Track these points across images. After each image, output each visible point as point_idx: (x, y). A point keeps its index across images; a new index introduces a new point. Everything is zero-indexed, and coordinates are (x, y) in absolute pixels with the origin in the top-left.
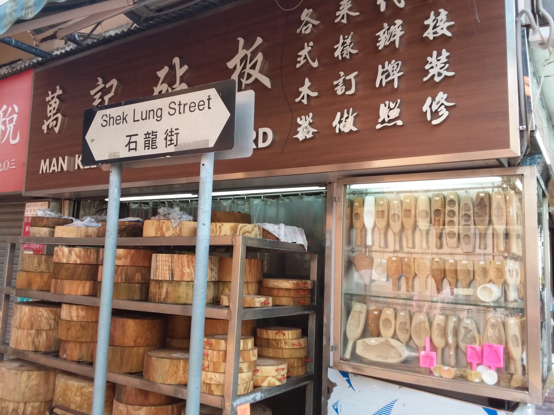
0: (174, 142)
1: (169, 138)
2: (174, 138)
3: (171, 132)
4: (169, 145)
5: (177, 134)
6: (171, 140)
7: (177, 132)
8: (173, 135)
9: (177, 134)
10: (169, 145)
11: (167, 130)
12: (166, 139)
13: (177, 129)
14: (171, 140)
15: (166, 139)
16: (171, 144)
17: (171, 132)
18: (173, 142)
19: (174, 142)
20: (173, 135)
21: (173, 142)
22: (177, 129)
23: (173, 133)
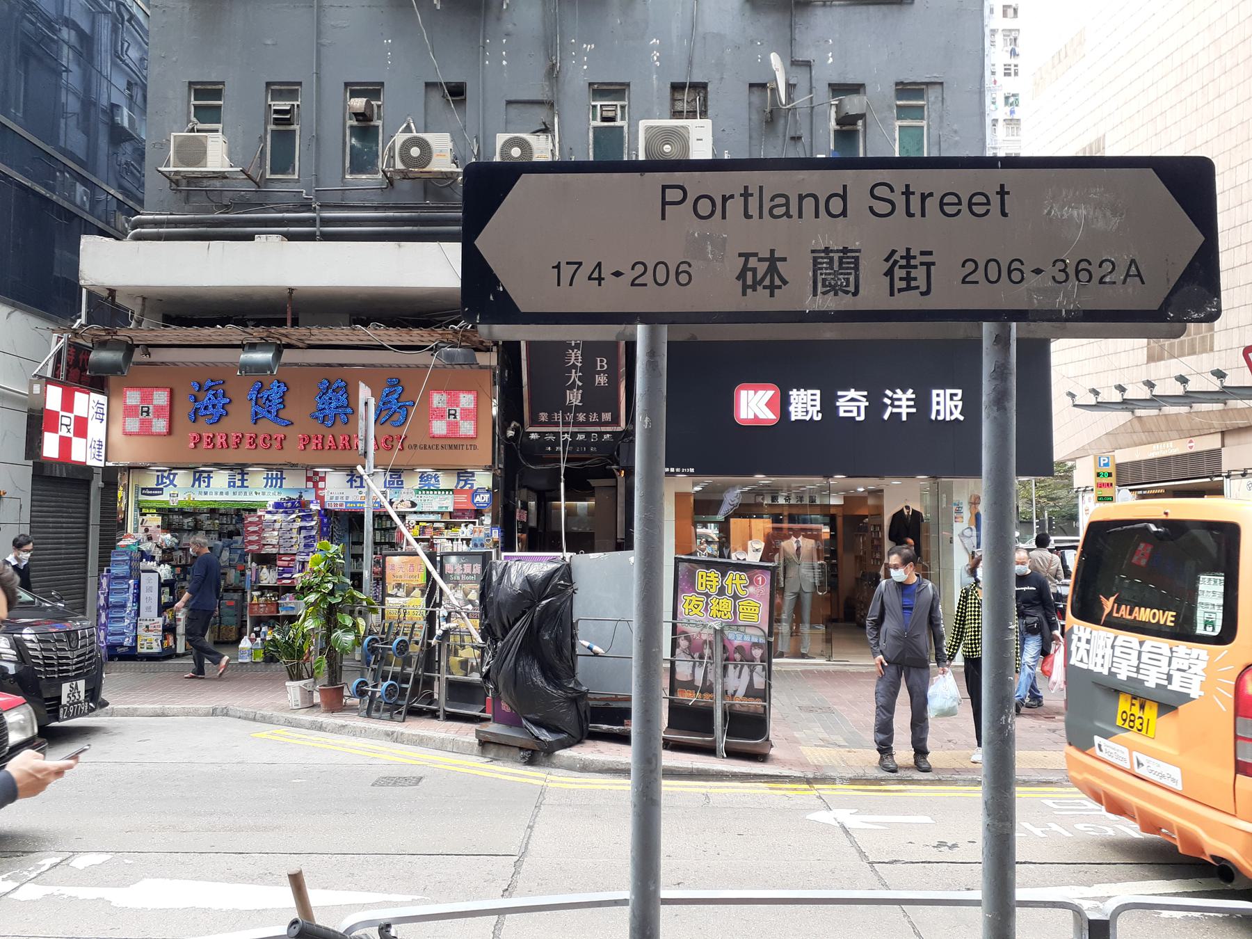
1: (899, 273)
2: (920, 273)
3: (908, 256)
4: (900, 290)
5: (929, 265)
6: (908, 279)
8: (915, 267)
9: (929, 265)
10: (900, 290)
11: (894, 252)
12: (890, 273)
14: (908, 279)
16: (909, 288)
17: (908, 256)
18: (913, 284)
20: (915, 267)
21: (913, 284)
23: (913, 262)
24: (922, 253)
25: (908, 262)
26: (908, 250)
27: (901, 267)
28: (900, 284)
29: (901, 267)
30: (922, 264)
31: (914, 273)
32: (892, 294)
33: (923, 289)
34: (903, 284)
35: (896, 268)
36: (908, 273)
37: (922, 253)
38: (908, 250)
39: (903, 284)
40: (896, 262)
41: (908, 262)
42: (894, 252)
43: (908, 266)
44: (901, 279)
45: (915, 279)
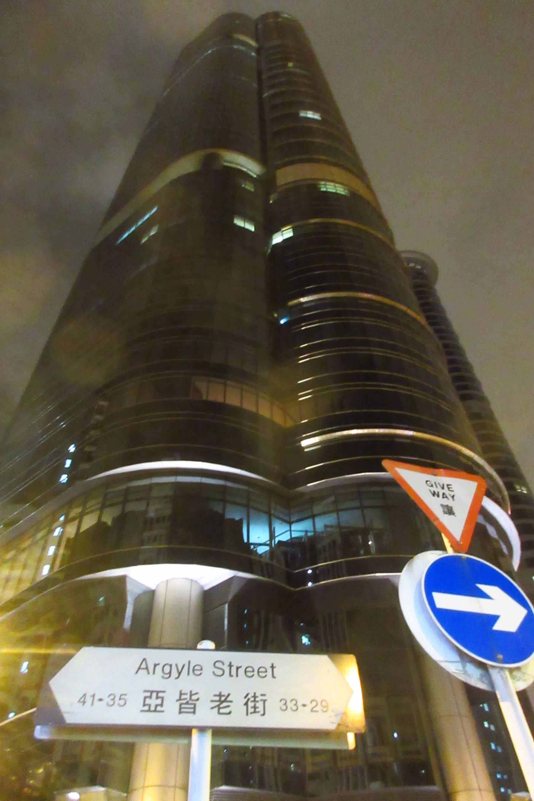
1: (251, 704)
2: (260, 705)
3: (255, 697)
4: (251, 713)
6: (255, 707)
7: (263, 698)
8: (258, 702)
9: (264, 701)
10: (251, 713)
11: (247, 695)
12: (246, 704)
15: (246, 704)
17: (255, 697)
18: (257, 710)
20: (258, 702)
23: (257, 699)
24: (262, 695)
25: (255, 699)
26: (255, 694)
27: (251, 701)
28: (251, 710)
29: (251, 701)
30: (262, 700)
31: (257, 705)
32: (247, 714)
33: (262, 712)
34: (252, 710)
35: (249, 702)
36: (255, 705)
37: (262, 695)
38: (255, 694)
39: (252, 710)
40: (248, 700)
41: (255, 699)
42: (247, 695)
43: (254, 701)
44: (252, 707)
45: (258, 708)
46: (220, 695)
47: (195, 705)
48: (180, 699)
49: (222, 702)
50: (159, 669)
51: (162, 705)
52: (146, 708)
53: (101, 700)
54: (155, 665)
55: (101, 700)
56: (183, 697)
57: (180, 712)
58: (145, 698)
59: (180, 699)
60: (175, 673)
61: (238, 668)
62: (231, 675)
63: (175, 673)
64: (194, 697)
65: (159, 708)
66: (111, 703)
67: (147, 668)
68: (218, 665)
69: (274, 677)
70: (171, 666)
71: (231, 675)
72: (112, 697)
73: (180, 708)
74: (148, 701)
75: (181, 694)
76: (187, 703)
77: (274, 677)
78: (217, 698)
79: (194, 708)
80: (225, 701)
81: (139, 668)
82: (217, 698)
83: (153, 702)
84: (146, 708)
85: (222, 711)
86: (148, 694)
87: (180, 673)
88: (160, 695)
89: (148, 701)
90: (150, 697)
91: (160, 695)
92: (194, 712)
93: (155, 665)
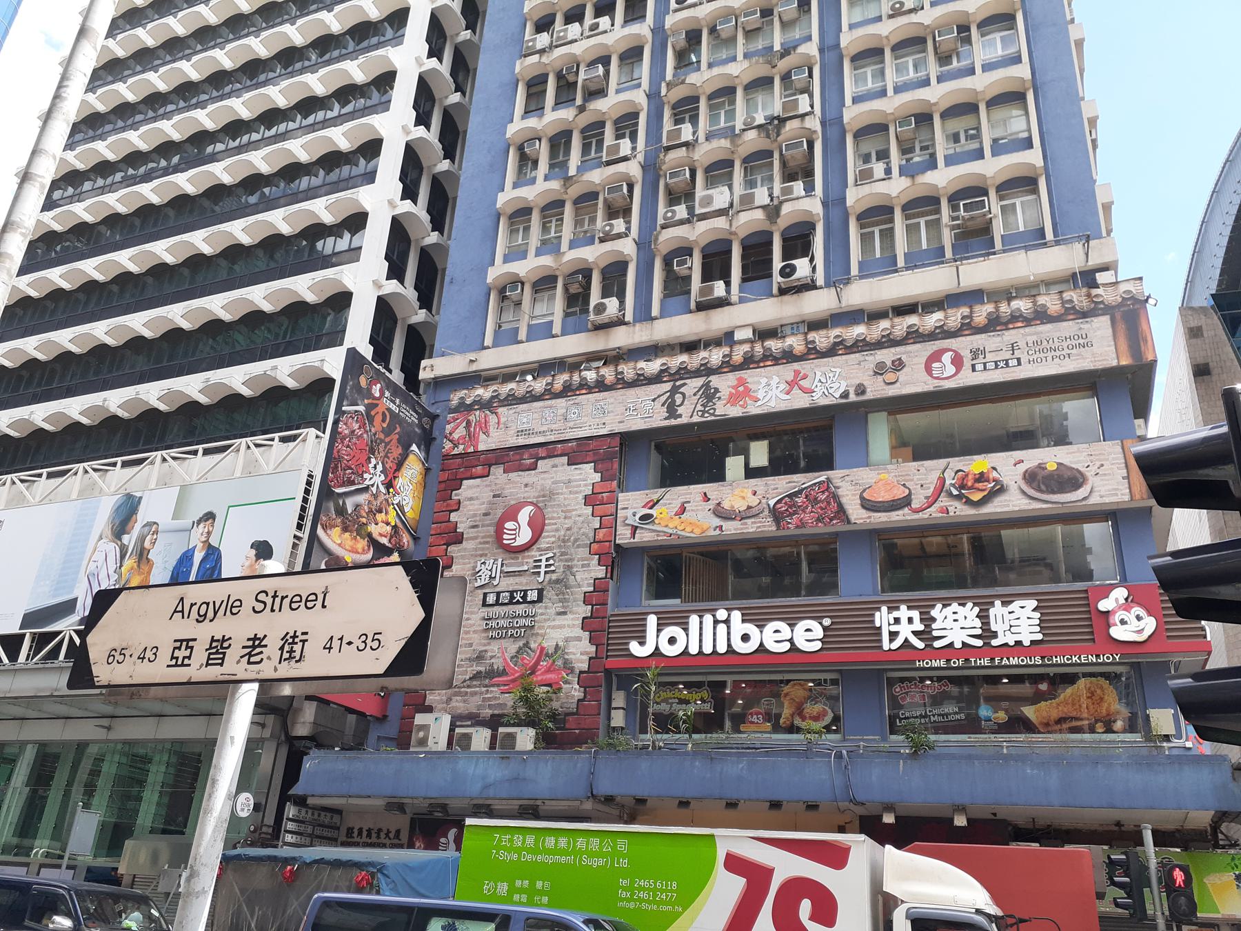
0: (297, 654)
1: (287, 648)
2: (297, 648)
3: (295, 636)
5: (304, 641)
6: (291, 651)
7: (304, 637)
9: (304, 641)
12: (282, 648)
13: (306, 633)
15: (282, 648)
19: (297, 654)
22: (306, 633)
31: (296, 647)
46: (255, 638)
47: (224, 654)
48: (211, 648)
49: (254, 647)
50: (195, 608)
51: (189, 658)
52: (174, 662)
53: (350, 643)
54: (192, 605)
55: (350, 643)
56: (214, 644)
57: (207, 664)
58: (175, 648)
59: (211, 648)
60: (210, 614)
61: (283, 598)
62: (272, 610)
63: (210, 614)
64: (225, 645)
65: (186, 661)
66: (362, 646)
67: (182, 611)
68: (262, 597)
69: (324, 606)
70: (208, 604)
71: (272, 610)
72: (364, 638)
73: (209, 659)
74: (177, 653)
75: (213, 640)
76: (217, 653)
77: (324, 606)
78: (250, 643)
79: (223, 659)
80: (260, 646)
81: (175, 611)
82: (250, 643)
83: (181, 654)
84: (174, 662)
85: (252, 659)
86: (178, 644)
87: (215, 613)
88: (191, 644)
89: (177, 653)
90: (179, 648)
91: (191, 644)
92: (221, 665)
93: (192, 605)
